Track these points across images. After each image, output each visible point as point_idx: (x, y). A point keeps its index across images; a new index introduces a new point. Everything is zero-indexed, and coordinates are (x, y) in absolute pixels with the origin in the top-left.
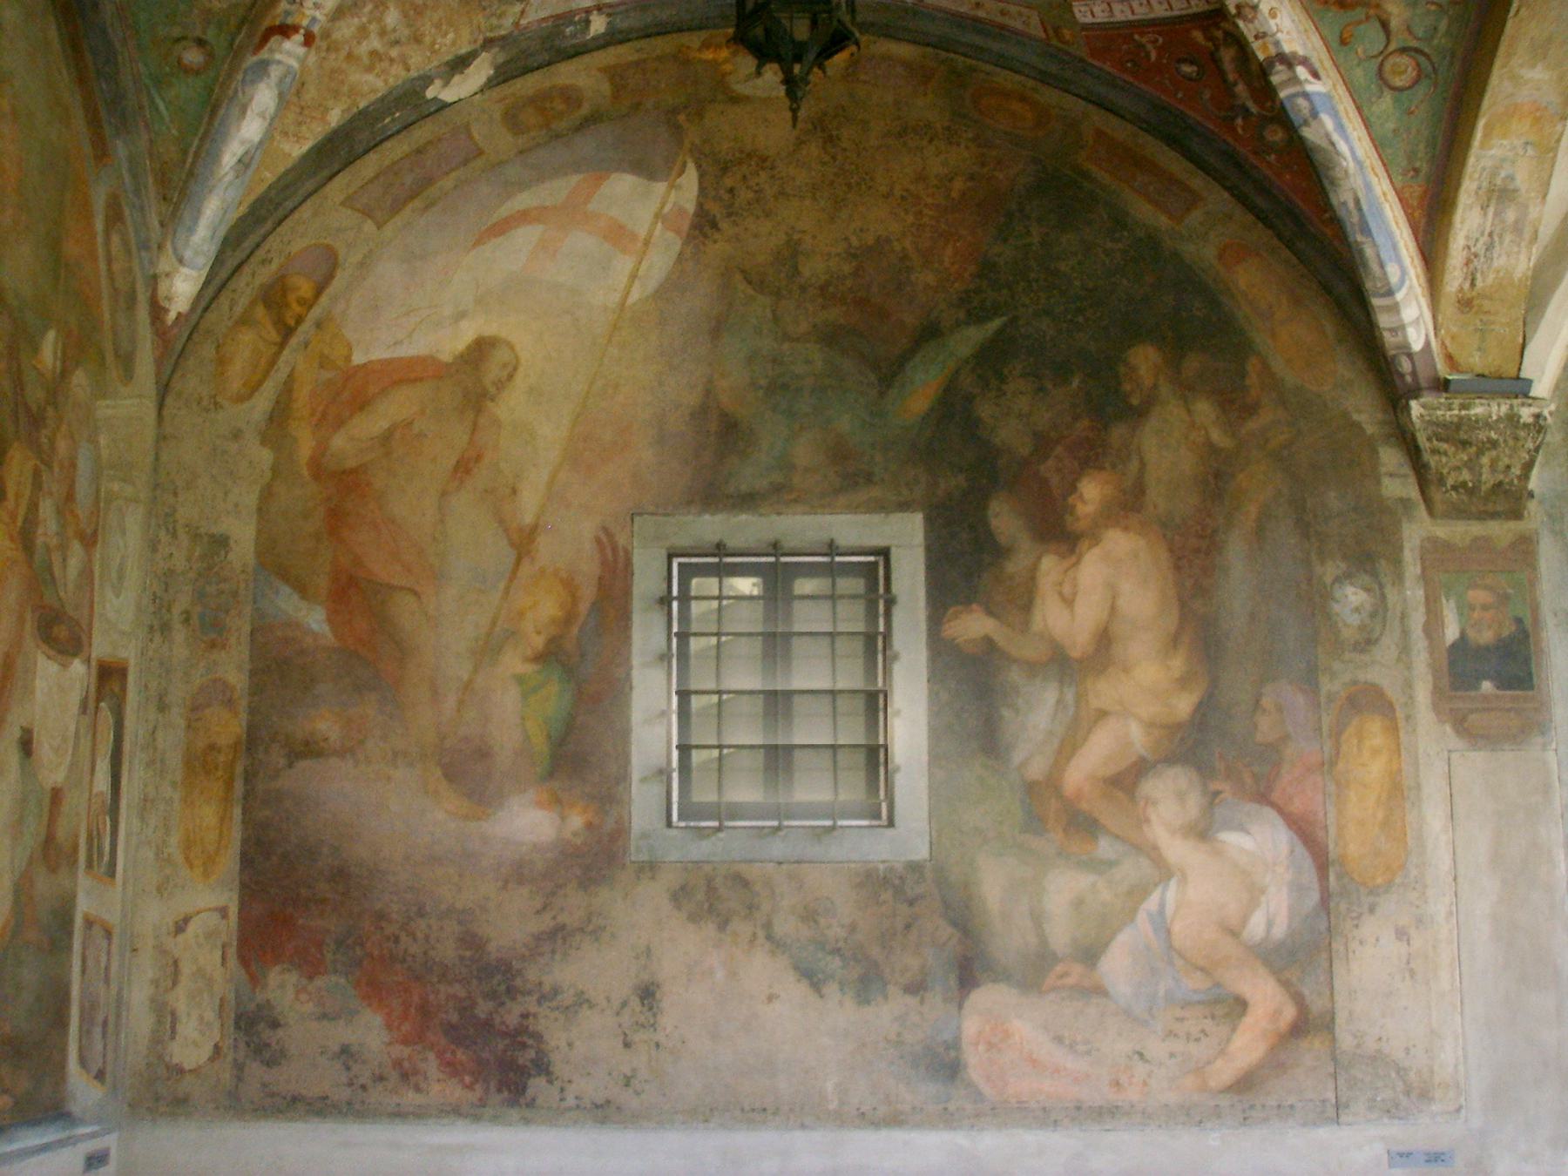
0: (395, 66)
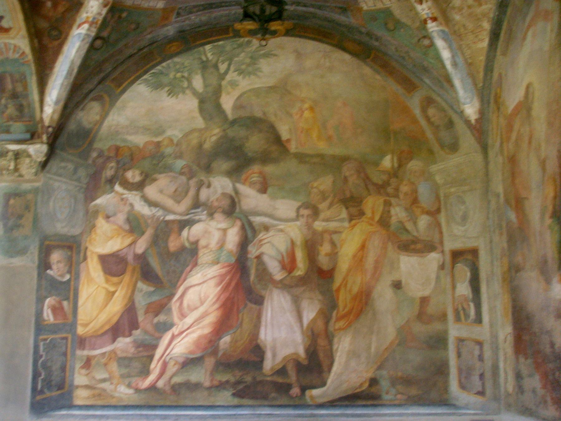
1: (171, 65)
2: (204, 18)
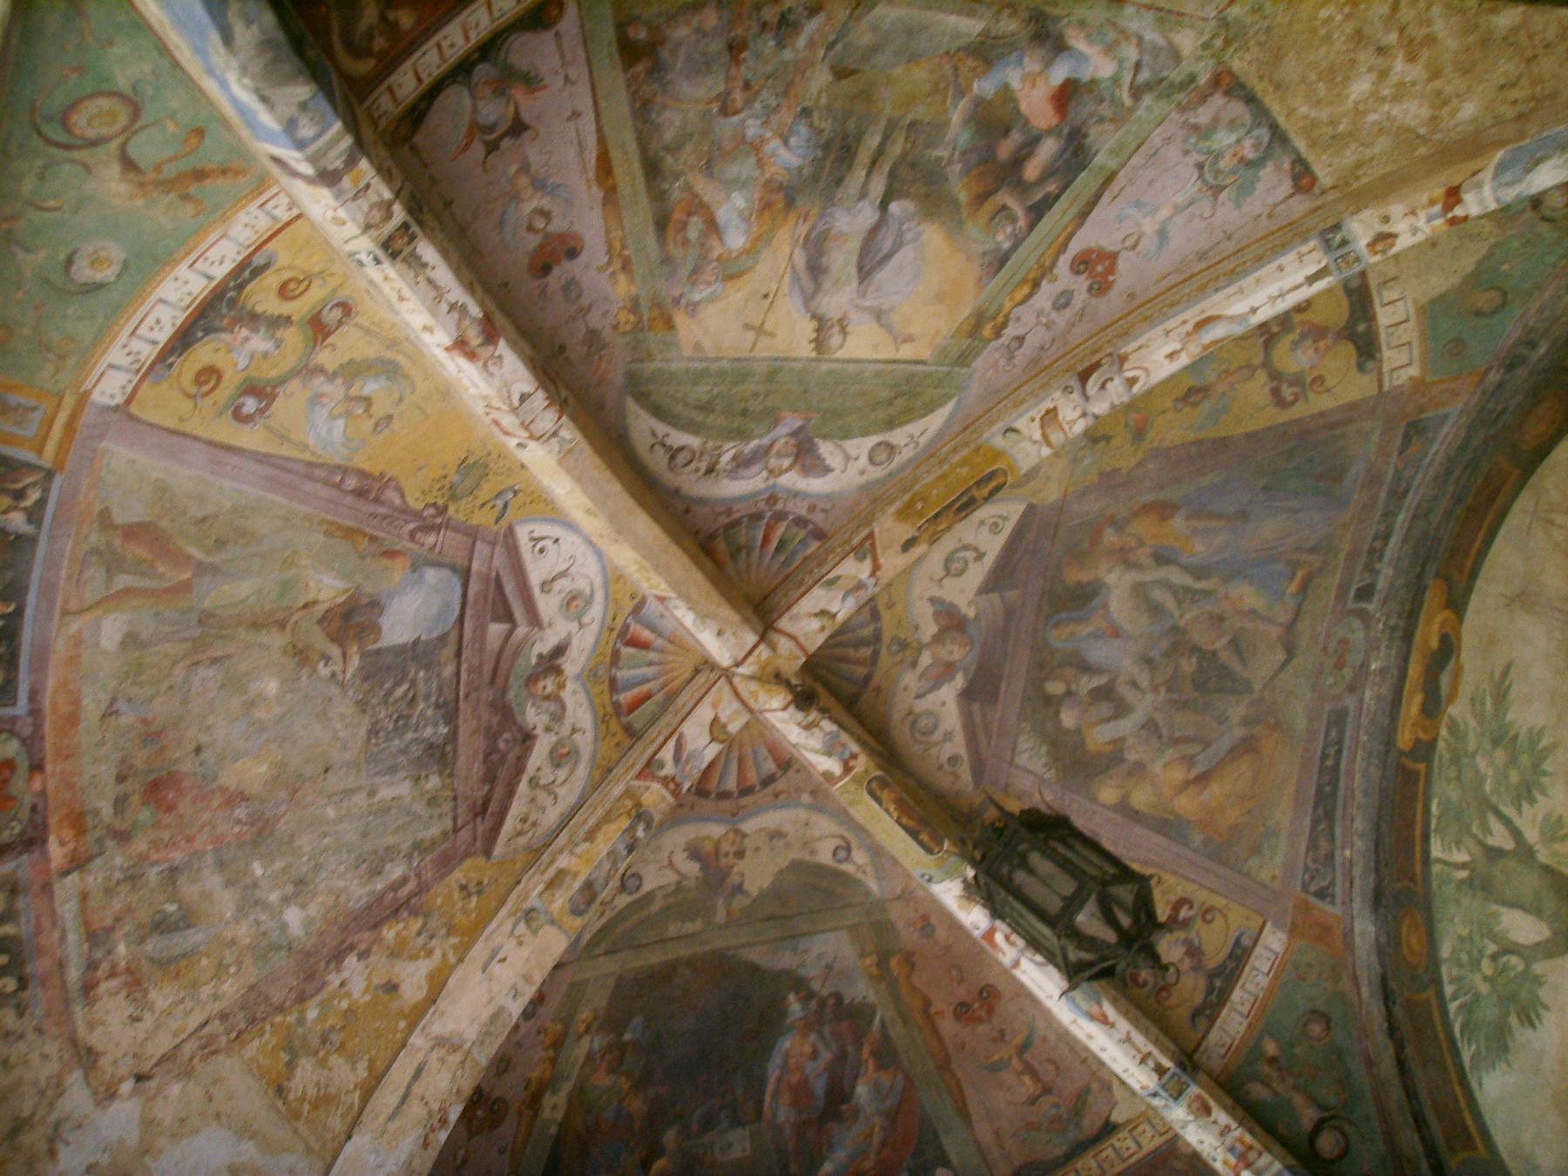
0: (1404, 20)
1: (1455, 972)
2: (1359, 824)
